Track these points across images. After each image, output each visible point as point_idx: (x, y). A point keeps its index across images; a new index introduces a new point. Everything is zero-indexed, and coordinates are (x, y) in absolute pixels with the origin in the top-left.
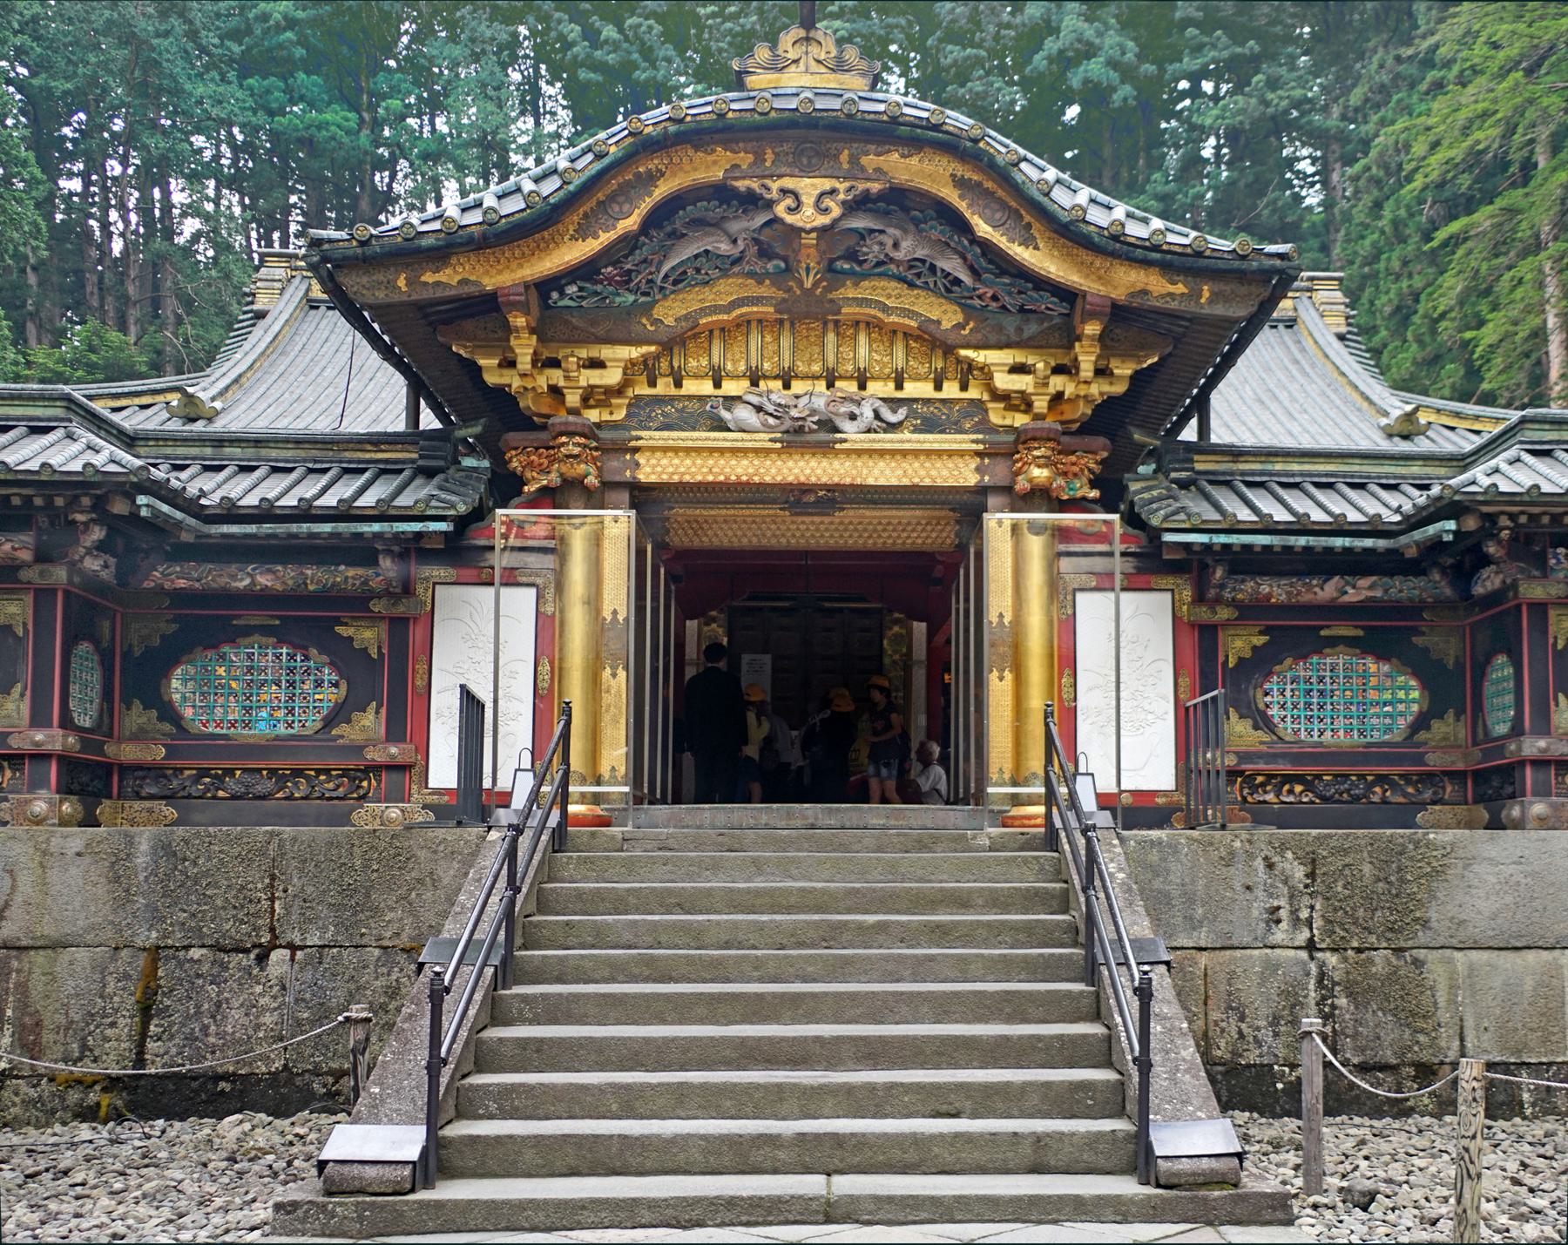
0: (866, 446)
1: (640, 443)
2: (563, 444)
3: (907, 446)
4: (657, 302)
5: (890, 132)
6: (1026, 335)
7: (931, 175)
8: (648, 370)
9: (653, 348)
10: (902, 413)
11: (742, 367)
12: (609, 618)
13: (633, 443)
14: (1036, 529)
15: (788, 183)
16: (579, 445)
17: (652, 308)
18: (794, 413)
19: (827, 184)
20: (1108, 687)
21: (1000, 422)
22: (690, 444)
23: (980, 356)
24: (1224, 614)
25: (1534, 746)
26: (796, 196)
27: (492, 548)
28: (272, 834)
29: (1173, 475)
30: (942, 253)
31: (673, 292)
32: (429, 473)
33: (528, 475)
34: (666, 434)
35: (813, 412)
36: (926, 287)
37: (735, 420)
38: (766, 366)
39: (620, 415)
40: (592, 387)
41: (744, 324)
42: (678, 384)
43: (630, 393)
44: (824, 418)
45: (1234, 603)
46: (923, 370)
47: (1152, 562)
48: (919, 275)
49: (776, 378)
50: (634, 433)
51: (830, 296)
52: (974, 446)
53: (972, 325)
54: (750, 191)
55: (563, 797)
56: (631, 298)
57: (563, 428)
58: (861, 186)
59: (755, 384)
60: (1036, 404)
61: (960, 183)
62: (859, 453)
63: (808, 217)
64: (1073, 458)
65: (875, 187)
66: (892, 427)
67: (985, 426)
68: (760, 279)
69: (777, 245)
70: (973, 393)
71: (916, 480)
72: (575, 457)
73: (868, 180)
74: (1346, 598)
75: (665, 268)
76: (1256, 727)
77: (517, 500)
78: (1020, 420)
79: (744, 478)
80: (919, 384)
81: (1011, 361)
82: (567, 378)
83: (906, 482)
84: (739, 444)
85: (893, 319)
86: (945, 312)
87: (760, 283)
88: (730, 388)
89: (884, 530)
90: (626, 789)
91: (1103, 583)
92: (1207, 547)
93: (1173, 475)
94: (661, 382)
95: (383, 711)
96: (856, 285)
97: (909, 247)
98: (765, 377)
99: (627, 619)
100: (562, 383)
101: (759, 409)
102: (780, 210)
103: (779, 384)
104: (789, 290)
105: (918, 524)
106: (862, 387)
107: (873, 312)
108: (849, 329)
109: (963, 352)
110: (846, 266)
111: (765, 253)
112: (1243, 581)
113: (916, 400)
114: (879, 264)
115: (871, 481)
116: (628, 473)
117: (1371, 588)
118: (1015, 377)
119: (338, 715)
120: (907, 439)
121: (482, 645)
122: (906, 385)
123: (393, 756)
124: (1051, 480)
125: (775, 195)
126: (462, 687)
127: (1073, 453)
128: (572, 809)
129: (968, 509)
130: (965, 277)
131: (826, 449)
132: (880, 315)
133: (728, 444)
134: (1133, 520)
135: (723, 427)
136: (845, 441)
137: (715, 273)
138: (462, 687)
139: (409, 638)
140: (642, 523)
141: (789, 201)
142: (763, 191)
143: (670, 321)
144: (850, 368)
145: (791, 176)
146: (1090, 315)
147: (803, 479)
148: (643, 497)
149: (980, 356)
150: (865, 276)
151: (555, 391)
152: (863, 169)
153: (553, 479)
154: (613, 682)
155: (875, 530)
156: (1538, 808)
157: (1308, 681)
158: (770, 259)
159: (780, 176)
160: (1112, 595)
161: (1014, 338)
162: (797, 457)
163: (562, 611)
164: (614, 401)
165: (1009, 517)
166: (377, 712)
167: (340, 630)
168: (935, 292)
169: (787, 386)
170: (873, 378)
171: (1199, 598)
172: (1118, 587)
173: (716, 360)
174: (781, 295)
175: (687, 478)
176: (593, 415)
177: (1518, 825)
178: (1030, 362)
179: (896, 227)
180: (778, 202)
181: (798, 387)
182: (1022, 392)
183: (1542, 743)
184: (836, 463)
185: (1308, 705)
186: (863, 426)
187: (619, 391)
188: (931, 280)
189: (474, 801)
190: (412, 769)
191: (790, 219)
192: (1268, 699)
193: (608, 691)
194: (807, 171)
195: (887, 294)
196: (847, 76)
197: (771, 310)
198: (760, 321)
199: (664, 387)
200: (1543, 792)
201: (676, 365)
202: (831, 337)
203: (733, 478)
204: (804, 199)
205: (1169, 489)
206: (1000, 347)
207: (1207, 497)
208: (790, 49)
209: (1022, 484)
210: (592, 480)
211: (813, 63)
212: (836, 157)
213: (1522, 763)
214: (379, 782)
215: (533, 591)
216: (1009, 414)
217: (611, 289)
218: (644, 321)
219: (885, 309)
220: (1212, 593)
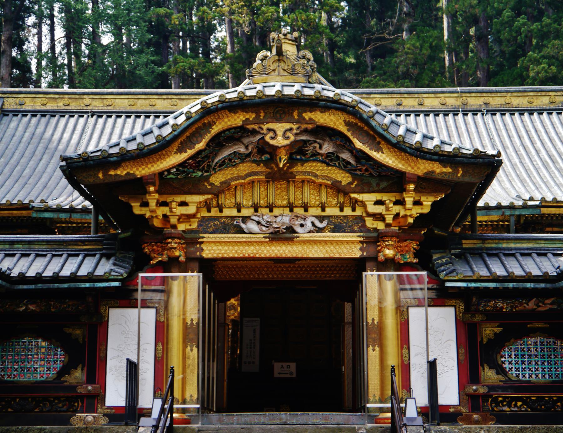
0: (308, 239)
1: (204, 240)
2: (169, 243)
3: (327, 239)
4: (211, 175)
6: (381, 187)
9: (210, 196)
10: (325, 223)
12: (189, 323)
13: (201, 240)
14: (390, 278)
15: (271, 126)
16: (176, 243)
17: (209, 178)
18: (275, 225)
19: (288, 126)
21: (371, 226)
22: (227, 239)
24: (478, 318)
26: (274, 131)
27: (137, 290)
28: (41, 429)
29: (453, 251)
30: (342, 150)
31: (219, 170)
32: (108, 257)
33: (153, 255)
34: (216, 235)
35: (284, 224)
36: (335, 166)
37: (248, 229)
38: (262, 202)
39: (194, 226)
40: (182, 215)
42: (221, 211)
43: (199, 216)
44: (288, 226)
45: (485, 313)
46: (335, 202)
47: (441, 296)
48: (331, 160)
49: (266, 207)
50: (201, 235)
51: (290, 171)
52: (359, 239)
53: (355, 183)
55: (171, 410)
56: (200, 173)
57: (170, 235)
58: (304, 126)
59: (256, 211)
60: (387, 219)
61: (348, 124)
62: (304, 242)
63: (280, 141)
64: (405, 244)
65: (310, 126)
66: (320, 230)
67: (364, 228)
68: (258, 163)
69: (267, 152)
70: (359, 212)
71: (332, 255)
72: (175, 248)
73: (306, 123)
74: (540, 309)
75: (216, 161)
76: (497, 373)
77: (146, 268)
79: (252, 255)
80: (332, 209)
81: (375, 199)
82: (171, 211)
83: (327, 256)
84: (249, 240)
85: (320, 180)
86: (344, 177)
87: (258, 165)
88: (245, 212)
89: (320, 270)
90: (198, 406)
92: (467, 288)
93: (453, 251)
94: (213, 210)
95: (85, 369)
96: (302, 165)
97: (327, 148)
98: (261, 207)
99: (198, 324)
100: (168, 214)
101: (258, 223)
102: (267, 138)
103: (268, 210)
104: (272, 168)
105: (337, 266)
106: (306, 210)
107: (311, 177)
109: (353, 195)
110: (298, 157)
112: (489, 302)
113: (331, 216)
114: (313, 155)
115: (311, 256)
116: (198, 254)
117: (551, 304)
118: (377, 206)
119: (65, 370)
120: (328, 236)
121: (129, 335)
122: (327, 209)
123: (89, 391)
124: (395, 255)
125: (265, 131)
126: (128, 360)
127: (405, 241)
128: (175, 415)
129: (358, 266)
130: (352, 162)
132: (313, 179)
133: (244, 240)
134: (433, 273)
135: (241, 231)
136: (298, 237)
137: (238, 161)
138: (128, 360)
140: (206, 280)
141: (271, 134)
142: (260, 130)
143: (217, 184)
144: (300, 202)
145: (272, 123)
146: (410, 182)
147: (279, 255)
150: (307, 161)
151: (165, 216)
152: (304, 119)
153: (165, 258)
154: (191, 354)
155: (316, 270)
157: (522, 350)
158: (263, 155)
159: (267, 123)
160: (424, 308)
161: (376, 189)
162: (276, 244)
163: (168, 320)
164: (192, 220)
165: (375, 273)
166: (82, 370)
167: (66, 329)
168: (339, 167)
169: (271, 211)
170: (311, 206)
171: (467, 310)
172: (427, 304)
173: (238, 200)
174: (268, 170)
175: (225, 255)
178: (384, 199)
179: (320, 139)
180: (266, 134)
181: (276, 211)
182: (380, 214)
184: (294, 247)
185: (523, 362)
186: (307, 230)
187: (194, 216)
188: (337, 163)
189: (132, 413)
190: (100, 396)
191: (272, 142)
192: (503, 359)
193: (189, 358)
194: (279, 120)
195: (318, 168)
196: (297, 76)
197: (264, 177)
198: (259, 181)
199: (214, 212)
201: (220, 202)
203: (247, 255)
204: (278, 133)
205: (451, 258)
206: (369, 192)
207: (468, 263)
208: (271, 65)
209: (381, 257)
210: (182, 259)
211: (282, 71)
212: (292, 113)
214: (83, 403)
215: (154, 311)
216: (375, 222)
217: (191, 170)
218: (206, 184)
219: (316, 176)
220: (473, 308)
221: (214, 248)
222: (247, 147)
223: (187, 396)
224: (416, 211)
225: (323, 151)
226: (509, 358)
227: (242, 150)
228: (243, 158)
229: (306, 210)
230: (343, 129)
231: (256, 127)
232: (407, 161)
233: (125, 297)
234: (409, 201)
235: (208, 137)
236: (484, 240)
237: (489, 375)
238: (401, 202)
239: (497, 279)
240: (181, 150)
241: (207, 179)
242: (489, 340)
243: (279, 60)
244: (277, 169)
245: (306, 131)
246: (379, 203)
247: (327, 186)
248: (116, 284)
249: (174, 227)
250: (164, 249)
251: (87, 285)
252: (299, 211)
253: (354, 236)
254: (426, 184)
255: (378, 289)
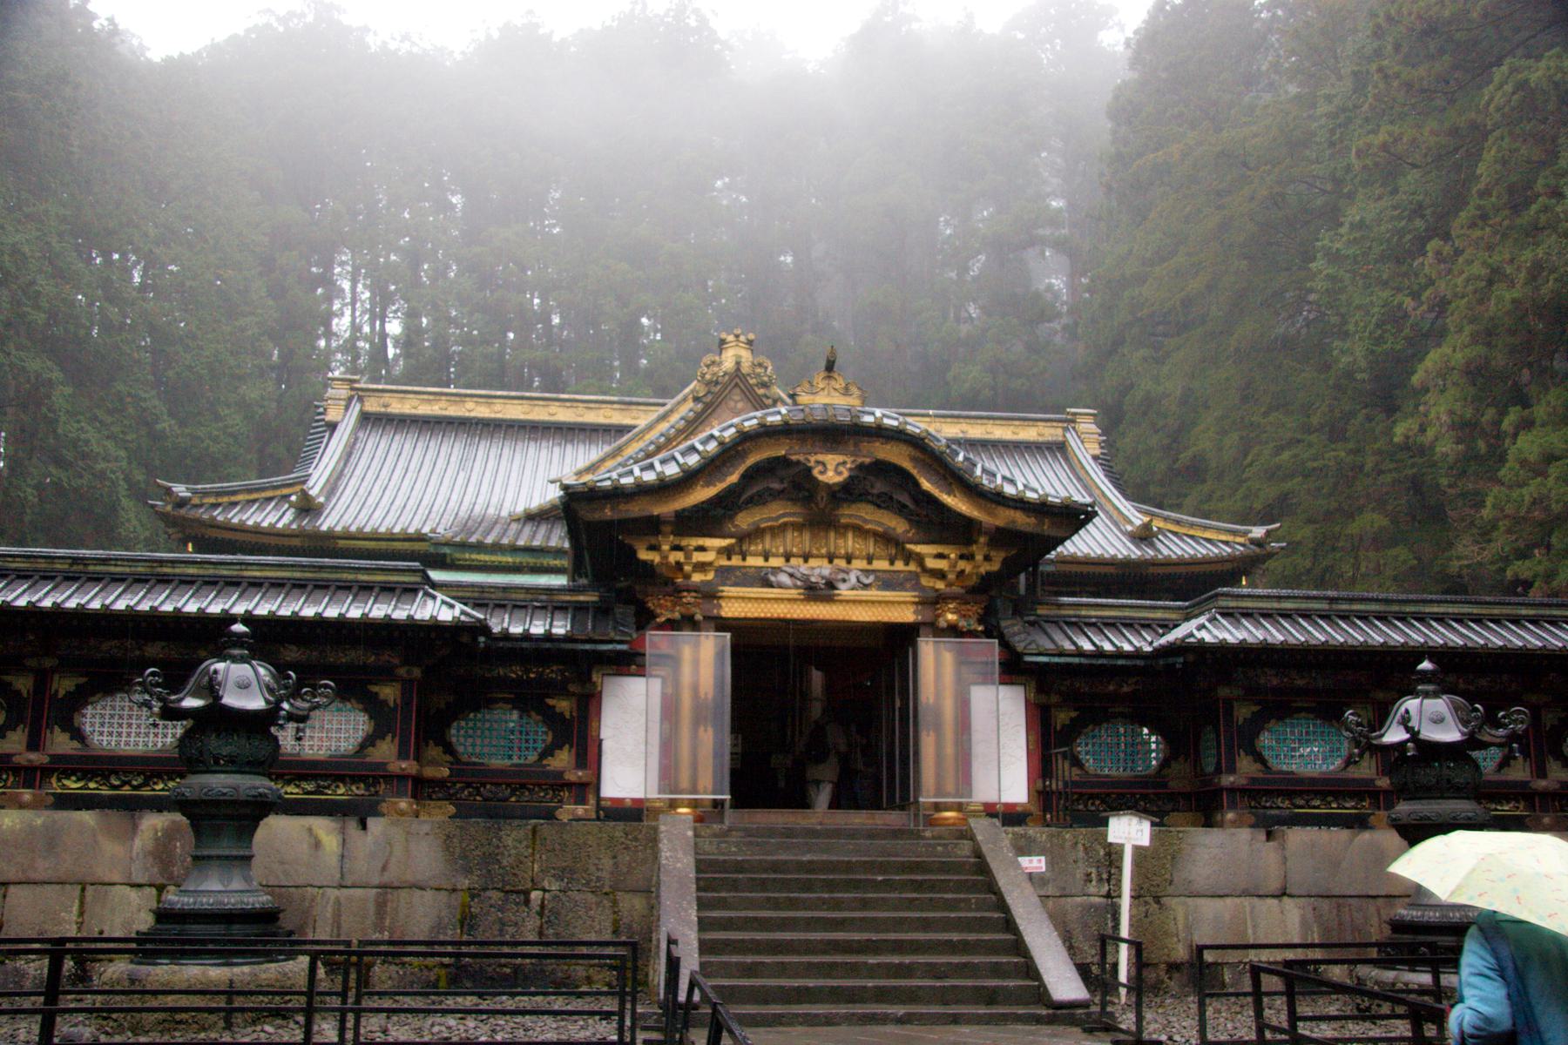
5: (879, 433)
7: (897, 455)
8: (728, 552)
11: (781, 550)
15: (820, 457)
19: (840, 458)
20: (986, 744)
23: (919, 549)
24: (1054, 699)
25: (1228, 780)
26: (824, 464)
36: (887, 508)
39: (710, 576)
41: (784, 527)
42: (744, 559)
47: (1013, 669)
54: (798, 462)
58: (860, 460)
59: (788, 560)
65: (867, 460)
66: (866, 587)
68: (794, 500)
78: (940, 585)
83: (874, 619)
88: (775, 562)
91: (985, 680)
101: (791, 575)
102: (815, 472)
106: (849, 562)
108: (842, 529)
109: (908, 546)
111: (797, 486)
131: (829, 599)
135: (771, 586)
139: (589, 705)
141: (820, 468)
148: (722, 624)
149: (919, 549)
153: (677, 615)
156: (1230, 816)
176: (697, 578)
177: (1221, 825)
183: (1232, 779)
191: (820, 478)
194: (831, 450)
199: (736, 561)
200: (1233, 806)
202: (832, 534)
209: (942, 623)
210: (699, 617)
213: (1222, 789)
219: (866, 521)
221: (739, 604)
222: (782, 481)
223: (700, 787)
224: (985, 568)
225: (875, 491)
226: (1083, 749)
227: (776, 486)
228: (777, 495)
229: (849, 562)
230: (907, 465)
231: (801, 458)
232: (980, 507)
233: (629, 663)
234: (979, 557)
235: (742, 469)
236: (1061, 606)
237: (1064, 769)
238: (969, 557)
239: (1080, 653)
240: (708, 484)
241: (732, 518)
242: (1063, 726)
243: (829, 377)
244: (821, 510)
245: (861, 467)
246: (940, 556)
247: (875, 534)
248: (624, 647)
249: (687, 577)
250: (675, 605)
251: (588, 647)
252: (842, 563)
253: (908, 596)
254: (1001, 537)
255: (935, 664)
